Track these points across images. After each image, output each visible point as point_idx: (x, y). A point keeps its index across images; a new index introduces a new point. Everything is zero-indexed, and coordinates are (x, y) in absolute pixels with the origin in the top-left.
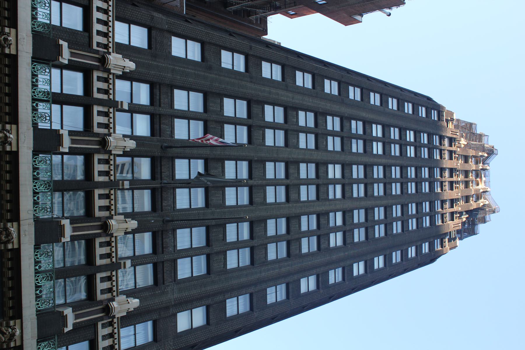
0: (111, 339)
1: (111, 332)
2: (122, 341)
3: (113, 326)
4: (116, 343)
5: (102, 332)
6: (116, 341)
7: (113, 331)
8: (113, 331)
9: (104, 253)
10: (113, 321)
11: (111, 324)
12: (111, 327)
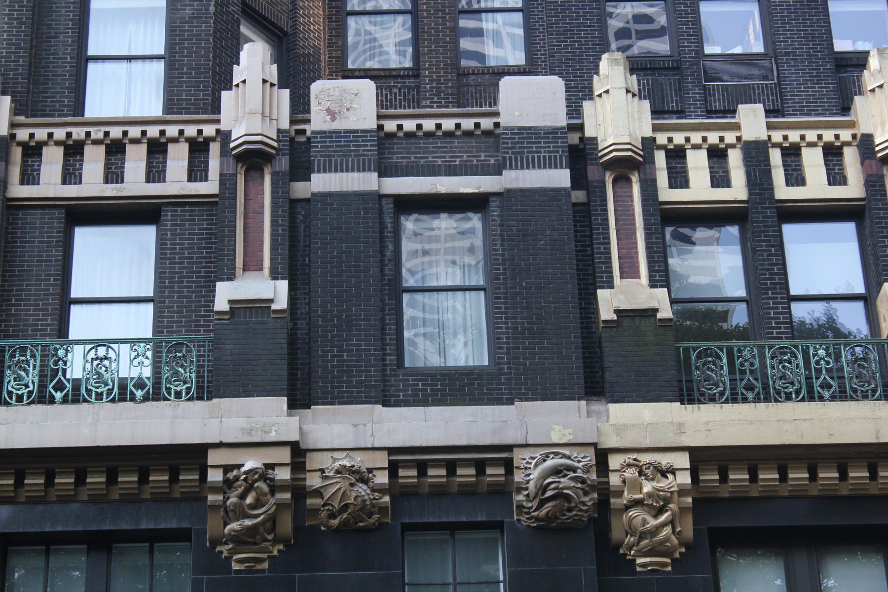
0: (88, 150)
1: (60, 151)
2: (136, 112)
3: (41, 145)
4: (101, 135)
5: (50, 183)
6: (134, 132)
7: (58, 143)
8: (96, 142)
9: (143, 165)
10: (24, 145)
11: (32, 151)
12: (45, 150)
